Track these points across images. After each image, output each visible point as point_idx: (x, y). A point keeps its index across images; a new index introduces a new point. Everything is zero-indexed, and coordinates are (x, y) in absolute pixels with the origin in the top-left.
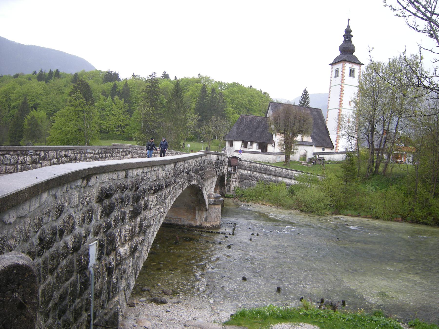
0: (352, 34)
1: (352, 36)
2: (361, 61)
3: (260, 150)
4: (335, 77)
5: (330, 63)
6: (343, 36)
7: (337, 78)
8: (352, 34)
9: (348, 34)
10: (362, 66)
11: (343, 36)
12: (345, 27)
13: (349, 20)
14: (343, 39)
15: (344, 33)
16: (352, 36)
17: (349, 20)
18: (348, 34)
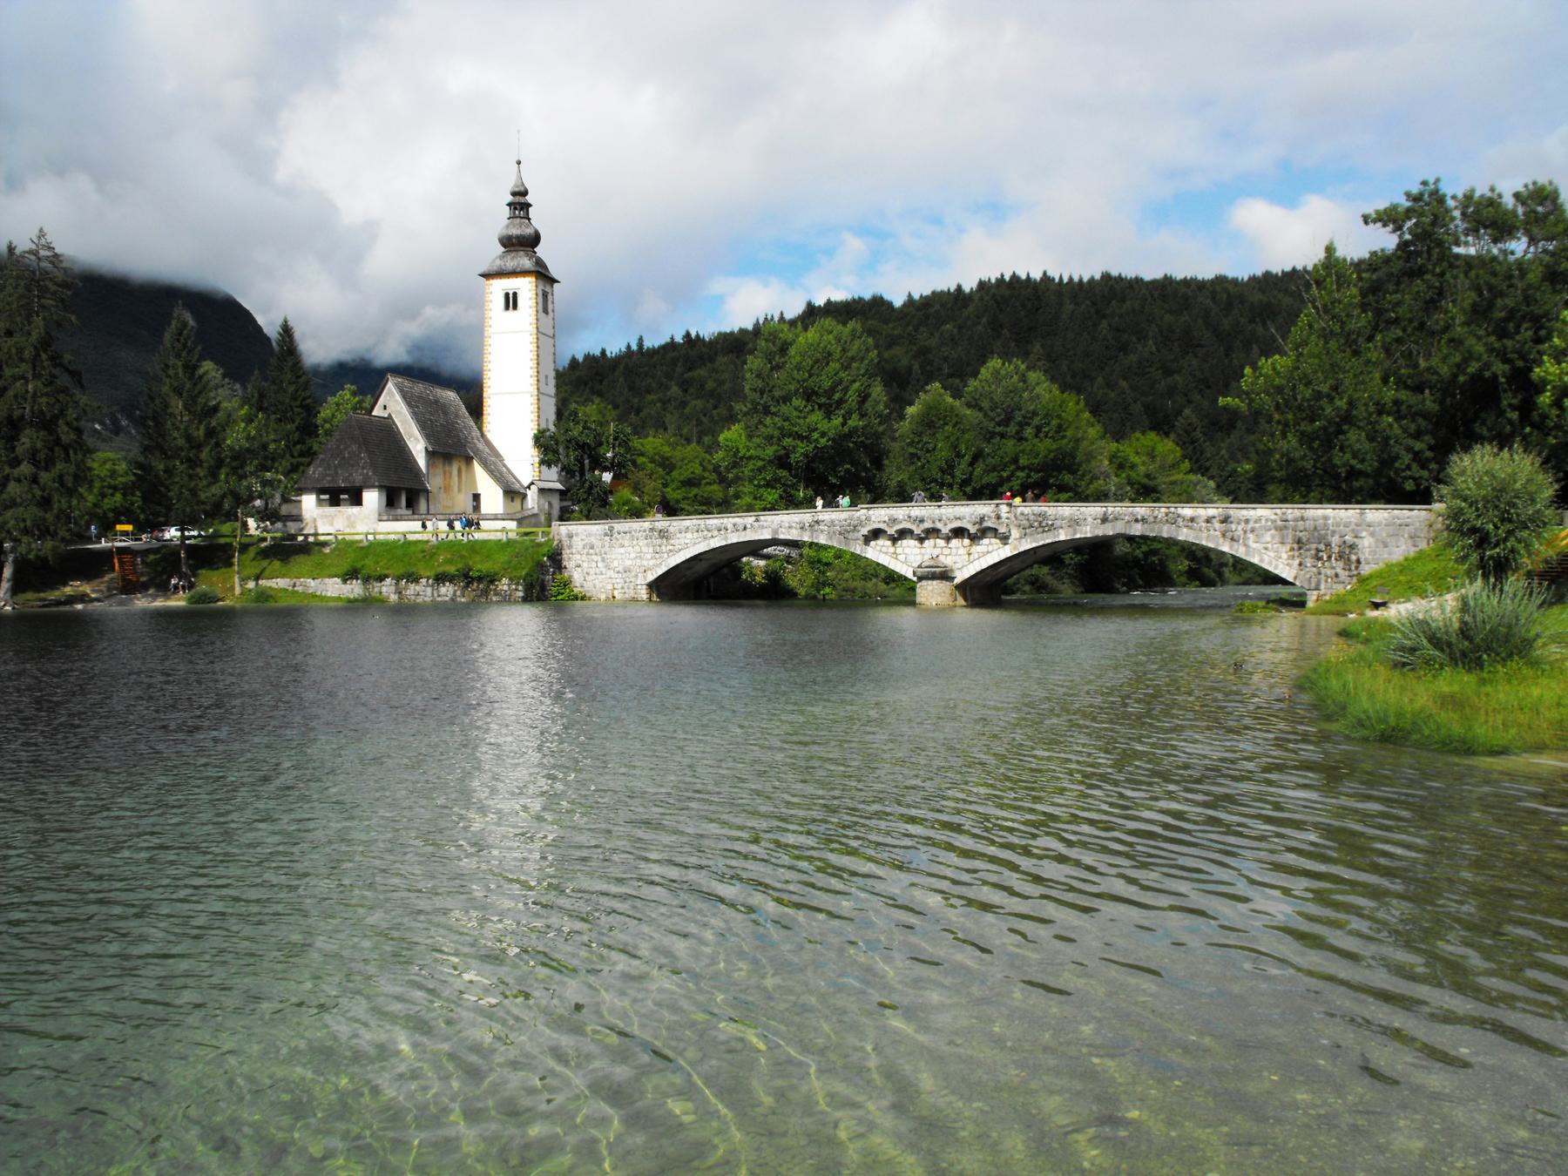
0: (529, 198)
1: (530, 205)
2: (554, 273)
3: (410, 512)
4: (507, 308)
5: (481, 271)
6: (509, 205)
7: (511, 312)
8: (529, 198)
9: (520, 205)
10: (556, 285)
11: (509, 205)
12: (510, 184)
13: (519, 163)
14: (506, 211)
15: (510, 198)
16: (530, 205)
17: (519, 163)
18: (520, 205)
